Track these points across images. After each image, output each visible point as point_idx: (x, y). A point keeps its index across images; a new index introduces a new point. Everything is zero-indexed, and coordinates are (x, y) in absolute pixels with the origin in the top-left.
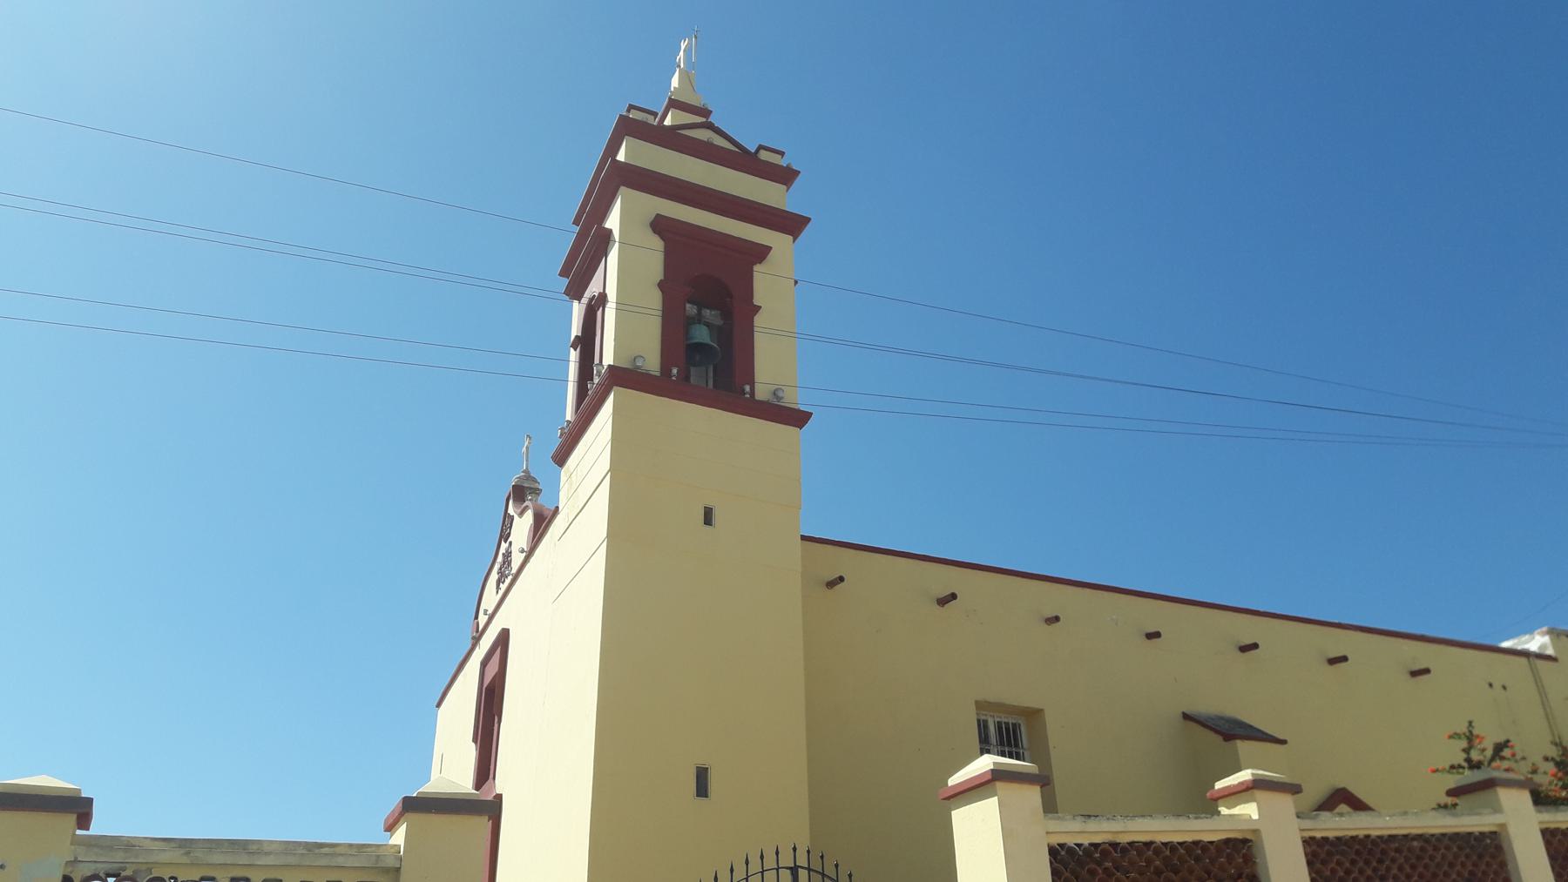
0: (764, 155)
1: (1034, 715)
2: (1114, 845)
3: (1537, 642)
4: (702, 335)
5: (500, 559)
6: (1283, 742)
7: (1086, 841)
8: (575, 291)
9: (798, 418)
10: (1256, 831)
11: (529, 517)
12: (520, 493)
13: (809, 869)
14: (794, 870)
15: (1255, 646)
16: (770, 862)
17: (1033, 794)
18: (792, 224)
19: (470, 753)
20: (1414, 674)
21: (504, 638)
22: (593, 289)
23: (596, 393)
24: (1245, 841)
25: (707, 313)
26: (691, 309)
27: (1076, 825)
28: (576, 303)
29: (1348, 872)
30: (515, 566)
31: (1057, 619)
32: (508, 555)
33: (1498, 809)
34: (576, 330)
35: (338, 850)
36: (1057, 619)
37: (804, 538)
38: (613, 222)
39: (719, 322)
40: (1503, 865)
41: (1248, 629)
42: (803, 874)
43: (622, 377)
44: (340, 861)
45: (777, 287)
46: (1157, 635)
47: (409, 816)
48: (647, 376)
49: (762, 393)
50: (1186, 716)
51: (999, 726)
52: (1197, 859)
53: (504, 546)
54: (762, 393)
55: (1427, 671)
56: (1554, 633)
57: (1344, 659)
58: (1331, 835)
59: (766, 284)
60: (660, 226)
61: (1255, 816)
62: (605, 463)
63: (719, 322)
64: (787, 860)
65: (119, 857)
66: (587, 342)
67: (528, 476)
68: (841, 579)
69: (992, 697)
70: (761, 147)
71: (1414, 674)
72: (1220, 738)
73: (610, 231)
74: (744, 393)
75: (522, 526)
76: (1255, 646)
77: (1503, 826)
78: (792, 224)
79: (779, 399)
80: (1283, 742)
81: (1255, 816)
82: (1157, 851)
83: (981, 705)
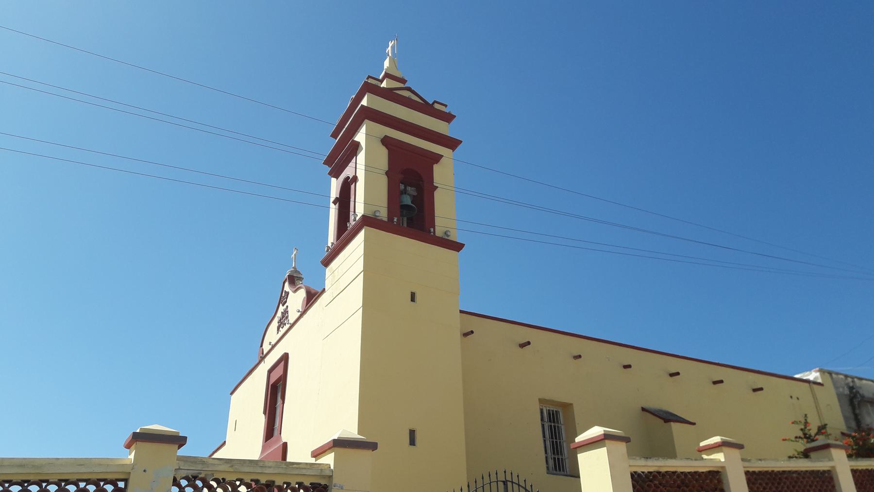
0: (437, 106)
1: (567, 407)
2: (659, 473)
3: (813, 375)
4: (407, 200)
5: (279, 314)
6: (694, 424)
7: (646, 470)
8: (336, 173)
9: (457, 247)
10: (723, 468)
11: (302, 294)
12: (293, 280)
13: (512, 482)
14: (505, 483)
16: (493, 478)
17: (622, 447)
18: (452, 143)
19: (261, 421)
20: (755, 390)
21: (285, 358)
22: (348, 172)
23: (353, 229)
24: (718, 472)
25: (409, 188)
26: (402, 187)
27: (642, 462)
28: (334, 180)
29: (764, 488)
30: (292, 319)
31: (580, 356)
32: (285, 312)
33: (831, 459)
34: (334, 193)
35: (301, 466)
36: (580, 356)
37: (461, 312)
38: (361, 137)
39: (415, 194)
40: (834, 487)
41: (675, 365)
42: (509, 484)
43: (368, 221)
44: (304, 472)
45: (443, 174)
46: (629, 366)
47: (336, 449)
48: (382, 221)
49: (439, 232)
50: (643, 409)
51: (549, 412)
52: (697, 480)
53: (282, 309)
54: (439, 232)
55: (761, 389)
56: (822, 371)
57: (721, 382)
58: (757, 470)
59: (442, 174)
60: (386, 141)
61: (723, 460)
62: (360, 266)
63: (415, 194)
64: (501, 477)
65: (199, 467)
66: (344, 201)
67: (296, 271)
68: (472, 332)
69: (547, 396)
70: (435, 102)
71: (755, 390)
72: (662, 421)
73: (358, 144)
74: (430, 232)
75: (296, 299)
76: (678, 374)
77: (833, 467)
78: (452, 143)
79: (448, 236)
80: (694, 424)
81: (723, 460)
82: (678, 476)
83: (541, 401)
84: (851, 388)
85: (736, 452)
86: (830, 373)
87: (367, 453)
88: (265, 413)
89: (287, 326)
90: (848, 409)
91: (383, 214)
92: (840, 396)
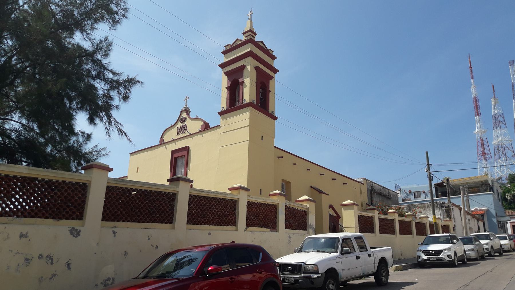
15: (323, 175)
20: (344, 184)
39: (261, 92)
43: (250, 104)
46: (309, 170)
49: (270, 111)
50: (311, 187)
60: (257, 68)
62: (248, 123)
71: (344, 184)
72: (318, 193)
83: (283, 180)
84: (372, 187)
85: (313, 204)
86: (367, 180)
87: (313, 204)
88: (171, 169)
89: (187, 134)
90: (369, 194)
91: (255, 103)
92: (368, 189)
